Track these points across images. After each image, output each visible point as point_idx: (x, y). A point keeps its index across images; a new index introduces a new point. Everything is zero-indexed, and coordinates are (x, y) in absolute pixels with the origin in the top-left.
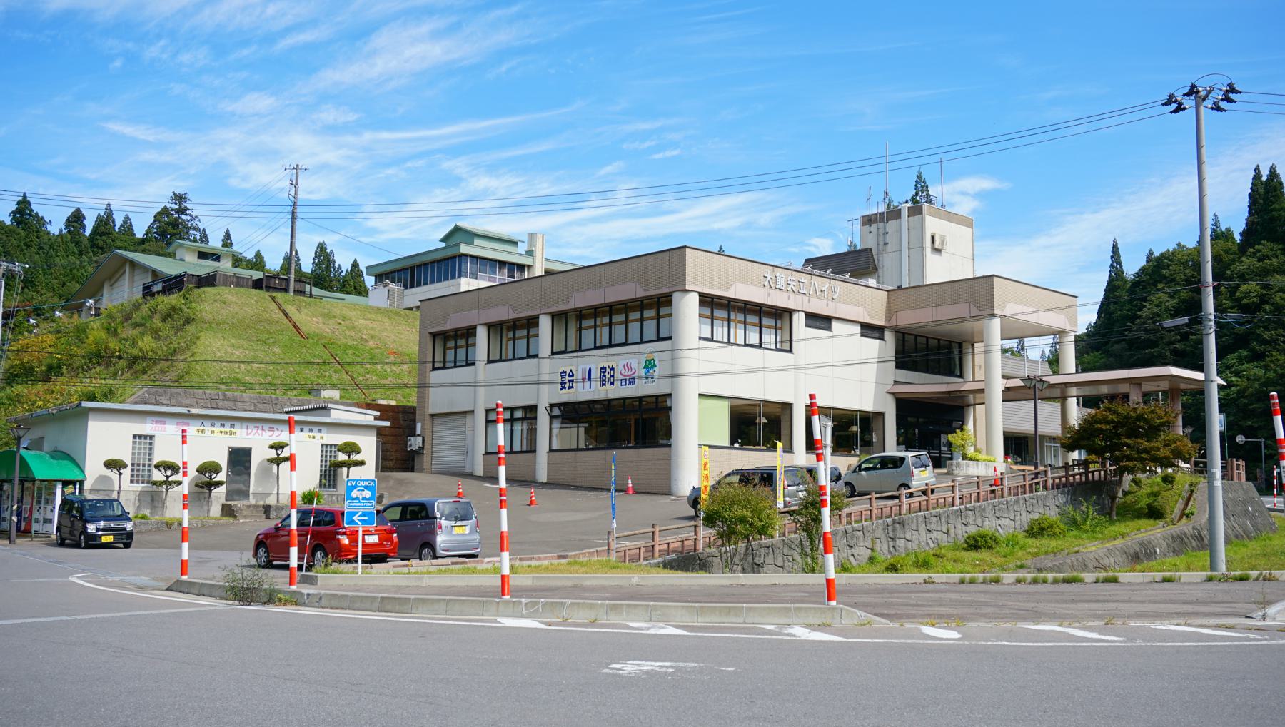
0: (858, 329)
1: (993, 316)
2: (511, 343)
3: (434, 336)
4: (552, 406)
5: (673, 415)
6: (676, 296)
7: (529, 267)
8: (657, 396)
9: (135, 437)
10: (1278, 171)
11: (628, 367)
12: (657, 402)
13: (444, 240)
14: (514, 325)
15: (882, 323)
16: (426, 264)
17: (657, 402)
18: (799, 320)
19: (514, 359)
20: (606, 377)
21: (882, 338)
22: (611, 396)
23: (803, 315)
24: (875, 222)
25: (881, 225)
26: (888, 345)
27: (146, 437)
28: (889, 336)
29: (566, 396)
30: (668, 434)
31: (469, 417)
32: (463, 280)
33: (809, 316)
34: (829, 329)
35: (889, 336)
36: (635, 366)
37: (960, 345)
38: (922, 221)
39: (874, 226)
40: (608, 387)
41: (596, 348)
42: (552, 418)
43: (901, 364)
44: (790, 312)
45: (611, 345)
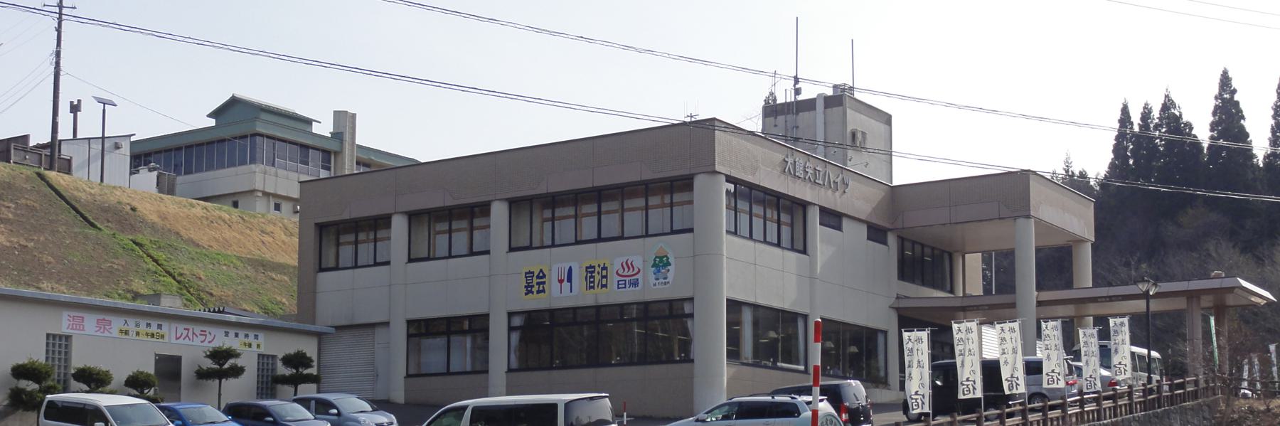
0: (863, 230)
1: (1028, 217)
2: (548, 225)
3: (322, 228)
4: (511, 315)
5: (1017, 275)
6: (699, 181)
7: (336, 153)
8: (670, 302)
9: (48, 335)
10: (1230, 74)
11: (630, 266)
12: (671, 308)
13: (215, 114)
14: (448, 214)
15: (887, 225)
16: (200, 145)
17: (671, 308)
18: (814, 216)
19: (356, 266)
20: (594, 276)
21: (884, 242)
22: (603, 300)
23: (817, 209)
24: (783, 113)
25: (789, 117)
26: (888, 254)
27: (60, 337)
28: (892, 240)
29: (535, 302)
30: (686, 346)
31: (380, 333)
32: (257, 168)
33: (824, 211)
34: (839, 228)
35: (892, 240)
36: (638, 263)
37: (951, 255)
38: (845, 114)
39: (781, 119)
40: (598, 290)
41: (577, 242)
42: (511, 329)
43: (902, 276)
44: (804, 205)
45: (599, 239)
